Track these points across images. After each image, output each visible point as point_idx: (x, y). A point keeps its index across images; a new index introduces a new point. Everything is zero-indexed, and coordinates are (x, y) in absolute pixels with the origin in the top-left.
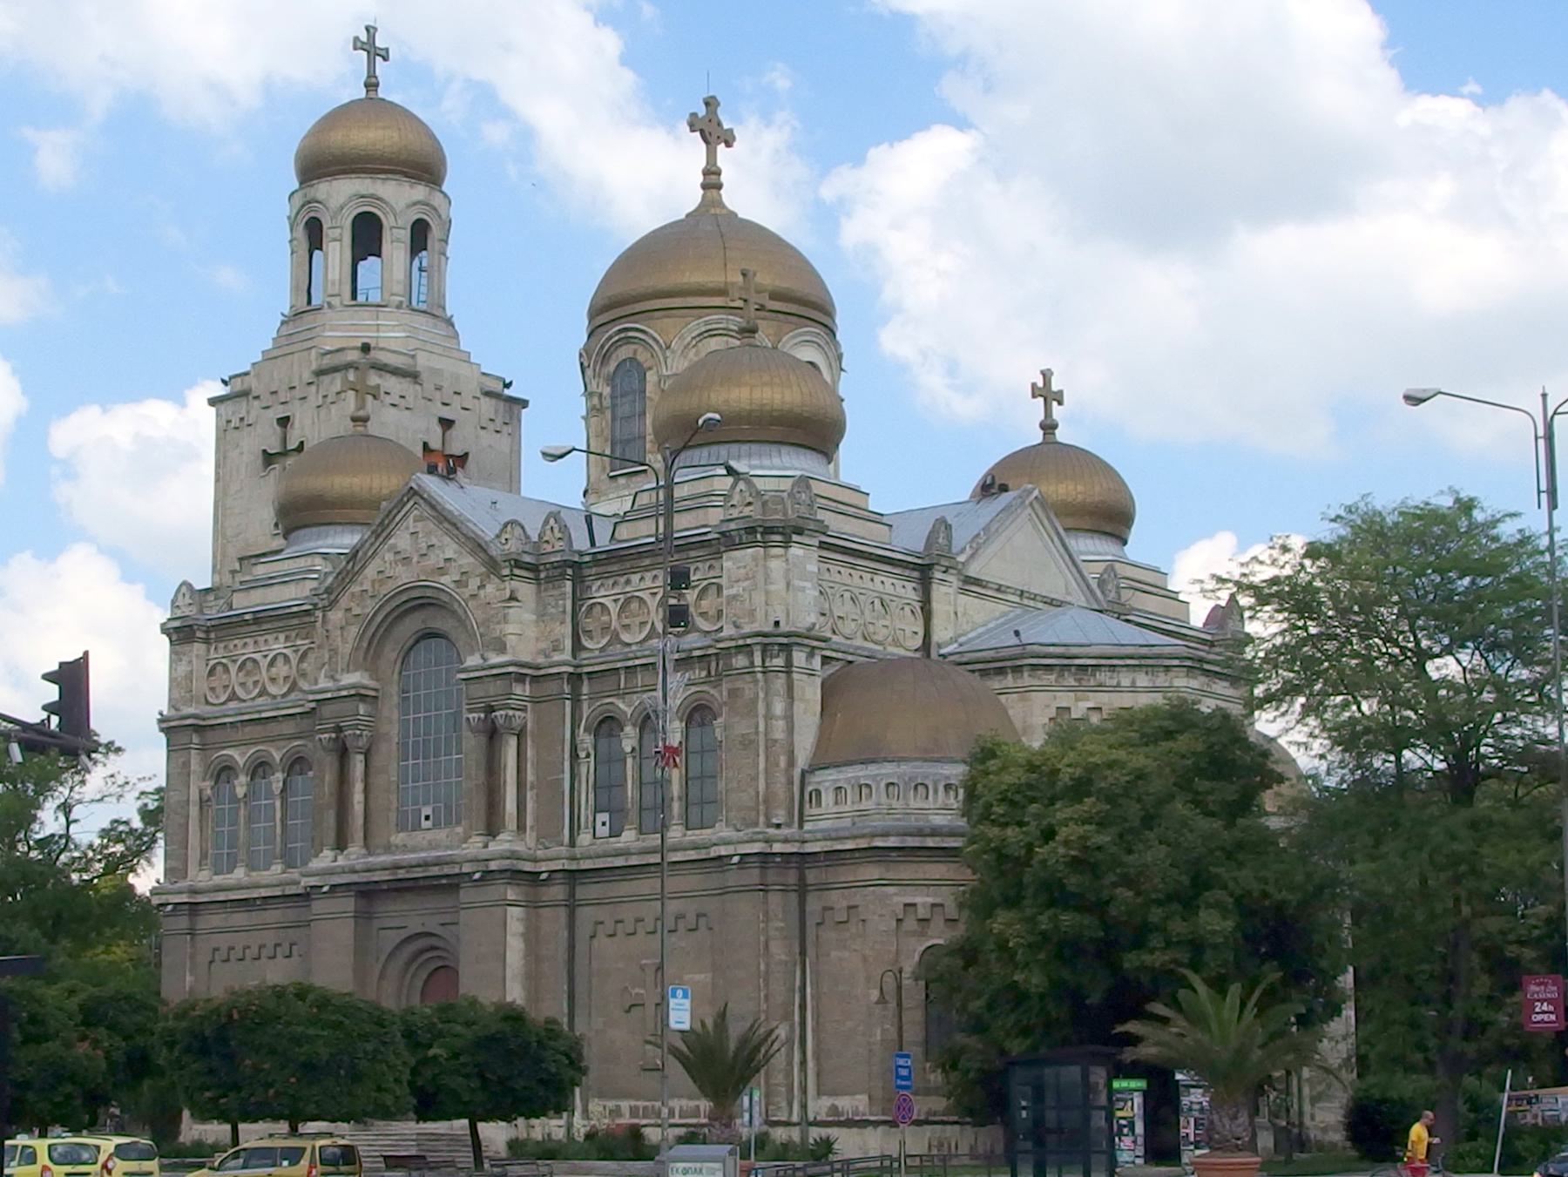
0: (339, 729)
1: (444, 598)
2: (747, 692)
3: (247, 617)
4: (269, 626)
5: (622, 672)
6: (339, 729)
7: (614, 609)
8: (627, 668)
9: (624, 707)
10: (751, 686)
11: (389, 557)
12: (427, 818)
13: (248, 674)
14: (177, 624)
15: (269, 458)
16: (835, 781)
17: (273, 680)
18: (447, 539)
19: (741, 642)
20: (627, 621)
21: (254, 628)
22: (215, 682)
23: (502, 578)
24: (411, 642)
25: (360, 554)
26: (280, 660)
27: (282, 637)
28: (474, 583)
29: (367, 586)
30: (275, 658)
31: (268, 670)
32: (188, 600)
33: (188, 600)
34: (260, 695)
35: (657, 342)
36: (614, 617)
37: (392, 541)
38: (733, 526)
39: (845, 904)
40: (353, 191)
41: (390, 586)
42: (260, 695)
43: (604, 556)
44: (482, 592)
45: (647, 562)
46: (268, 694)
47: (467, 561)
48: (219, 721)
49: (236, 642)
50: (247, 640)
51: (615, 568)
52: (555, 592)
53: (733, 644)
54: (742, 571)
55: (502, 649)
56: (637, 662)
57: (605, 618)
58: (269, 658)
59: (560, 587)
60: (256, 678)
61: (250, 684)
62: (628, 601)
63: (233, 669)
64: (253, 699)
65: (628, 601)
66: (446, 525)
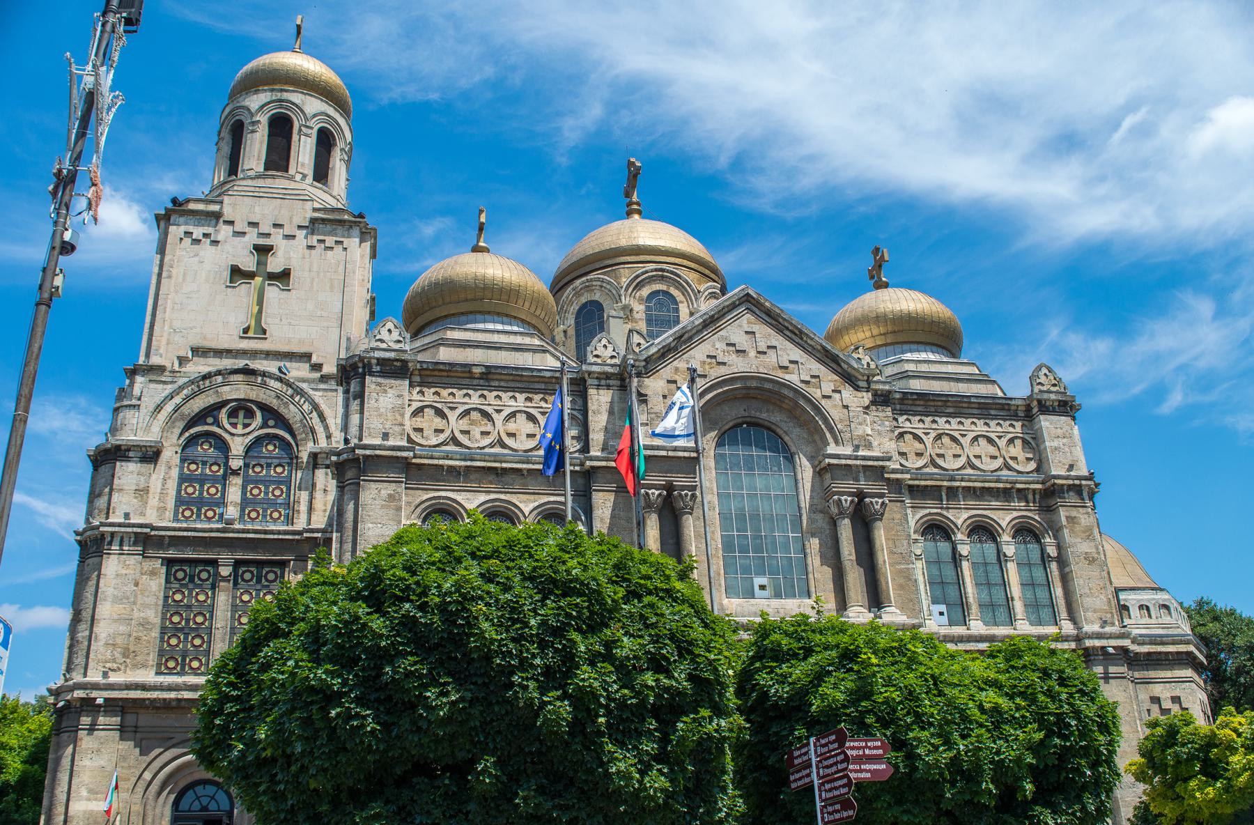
0: (670, 488)
1: (786, 392)
2: (1083, 521)
3: (477, 370)
4: (503, 384)
5: (960, 490)
6: (670, 488)
7: (928, 440)
8: (949, 488)
9: (960, 517)
10: (1086, 516)
11: (721, 346)
12: (762, 587)
13: (472, 423)
14: (392, 355)
15: (237, 273)
16: (1139, 600)
17: (511, 435)
18: (789, 345)
19: (1077, 482)
20: (941, 452)
21: (482, 382)
22: (418, 421)
23: (857, 388)
24: (731, 424)
25: (686, 336)
26: (521, 418)
27: (521, 397)
28: (827, 388)
29: (695, 364)
30: (513, 415)
31: (504, 425)
32: (395, 335)
33: (395, 335)
34: (491, 445)
35: (690, 286)
36: (929, 445)
37: (721, 333)
38: (1053, 397)
39: (1169, 695)
40: (323, 110)
41: (722, 371)
42: (491, 445)
43: (915, 397)
44: (837, 396)
45: (951, 410)
46: (504, 446)
47: (815, 367)
48: (435, 462)
49: (450, 390)
50: (471, 392)
51: (919, 409)
52: (881, 414)
53: (1071, 482)
54: (1059, 431)
55: (869, 446)
56: (963, 484)
57: (922, 446)
58: (505, 414)
59: (883, 411)
60: (484, 429)
61: (476, 432)
62: (939, 437)
63: (451, 417)
64: (484, 448)
65: (939, 437)
66: (788, 333)
